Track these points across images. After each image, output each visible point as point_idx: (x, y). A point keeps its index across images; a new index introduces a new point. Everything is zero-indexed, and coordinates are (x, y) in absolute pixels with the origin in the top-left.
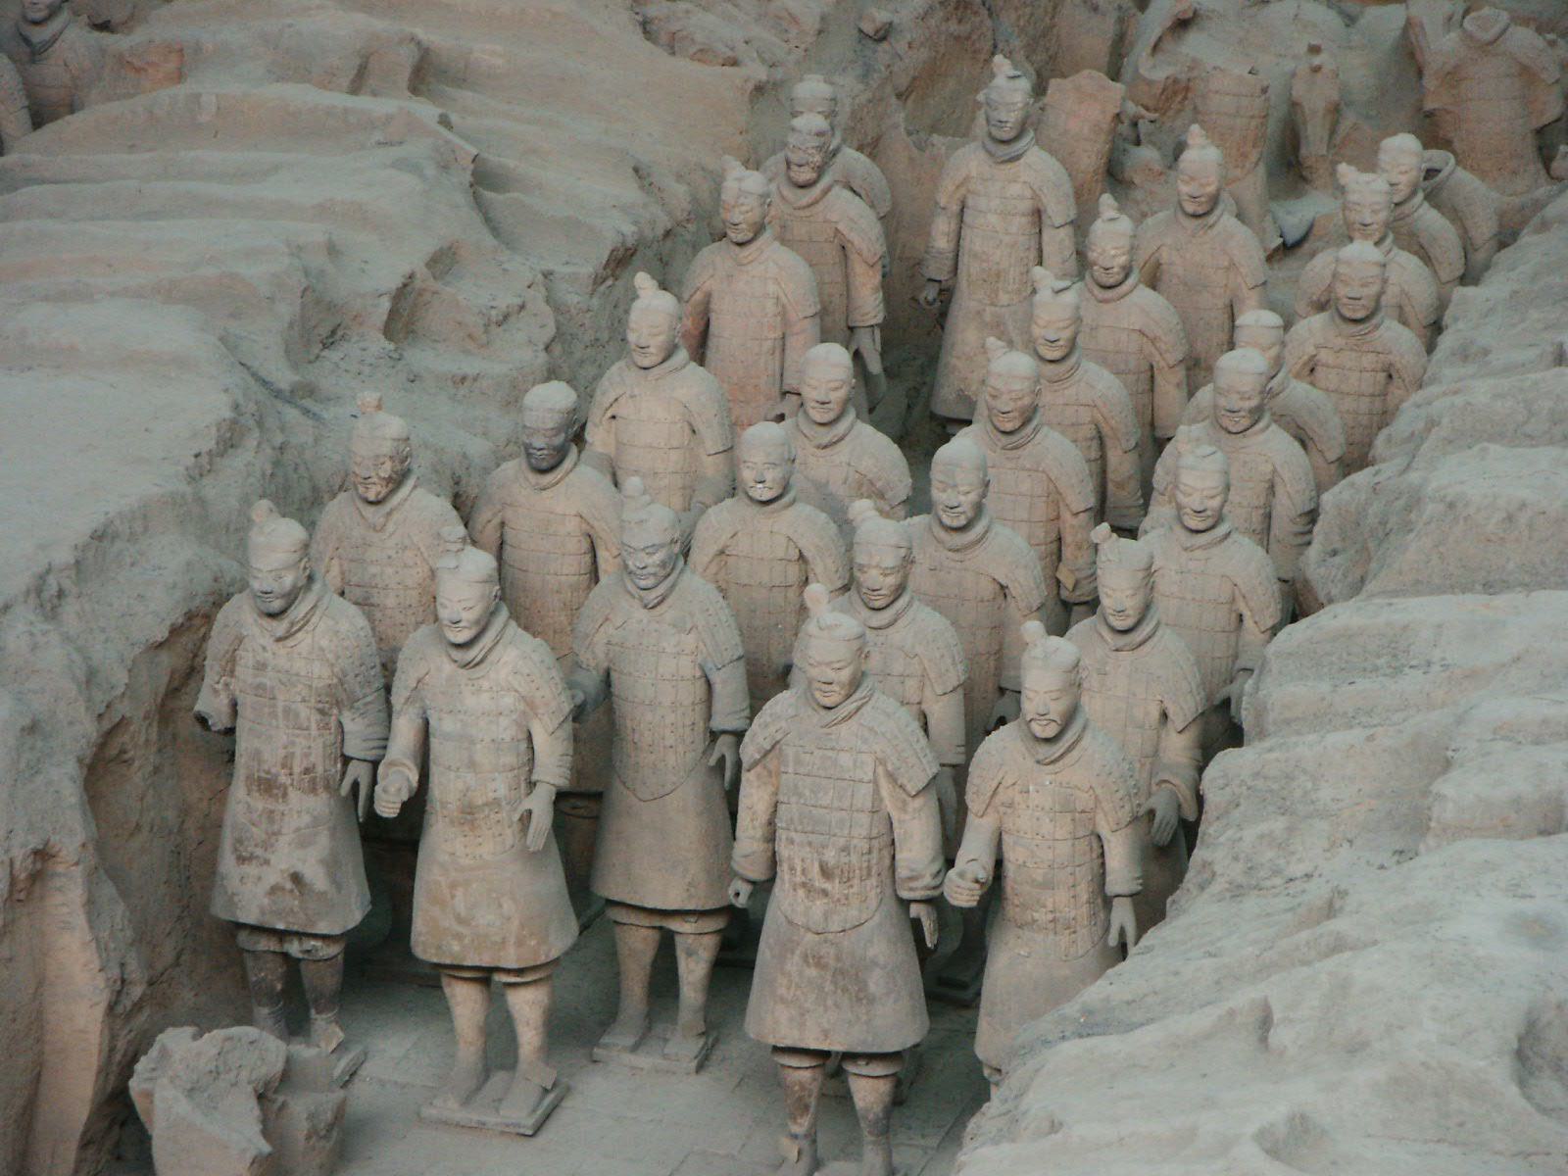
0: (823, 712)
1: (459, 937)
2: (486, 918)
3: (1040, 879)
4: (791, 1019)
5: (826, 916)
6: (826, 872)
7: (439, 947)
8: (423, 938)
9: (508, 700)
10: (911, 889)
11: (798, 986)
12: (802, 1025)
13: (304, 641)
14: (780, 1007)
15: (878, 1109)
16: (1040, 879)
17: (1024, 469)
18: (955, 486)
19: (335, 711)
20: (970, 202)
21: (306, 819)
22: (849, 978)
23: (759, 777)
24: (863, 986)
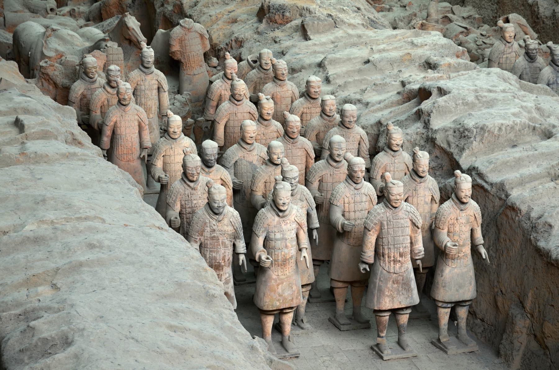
0: (393, 209)
1: (279, 300)
2: (287, 293)
3: (462, 244)
4: (389, 301)
5: (400, 268)
6: (401, 255)
7: (272, 305)
8: (267, 303)
9: (295, 226)
10: (419, 256)
11: (391, 291)
12: (393, 302)
13: (226, 221)
14: (386, 298)
15: (406, 323)
16: (462, 244)
17: (299, 148)
18: (341, 148)
19: (234, 240)
20: (138, 87)
21: (227, 275)
22: (406, 285)
23: (373, 232)
24: (410, 287)
